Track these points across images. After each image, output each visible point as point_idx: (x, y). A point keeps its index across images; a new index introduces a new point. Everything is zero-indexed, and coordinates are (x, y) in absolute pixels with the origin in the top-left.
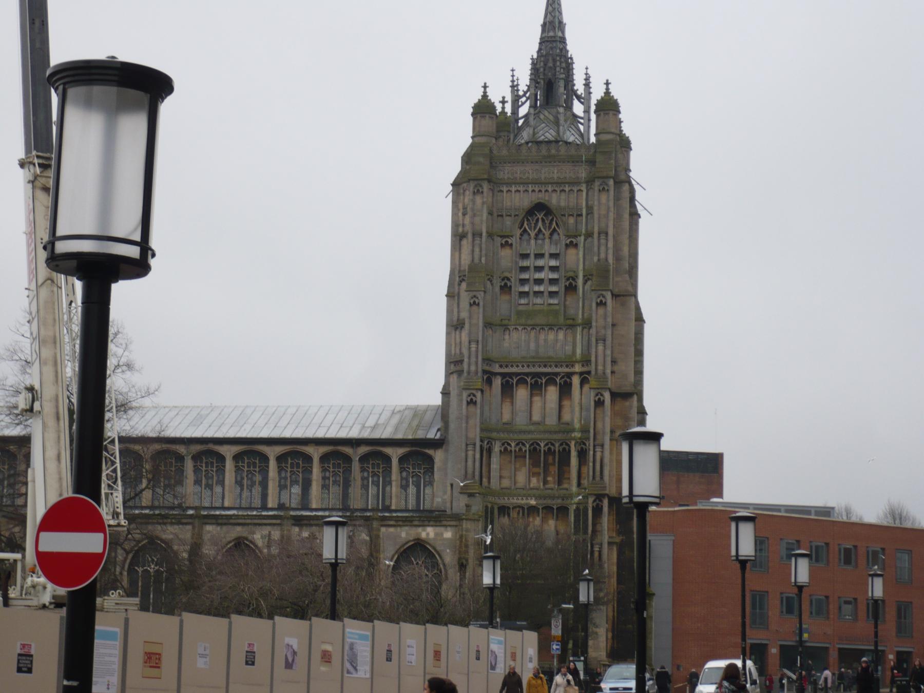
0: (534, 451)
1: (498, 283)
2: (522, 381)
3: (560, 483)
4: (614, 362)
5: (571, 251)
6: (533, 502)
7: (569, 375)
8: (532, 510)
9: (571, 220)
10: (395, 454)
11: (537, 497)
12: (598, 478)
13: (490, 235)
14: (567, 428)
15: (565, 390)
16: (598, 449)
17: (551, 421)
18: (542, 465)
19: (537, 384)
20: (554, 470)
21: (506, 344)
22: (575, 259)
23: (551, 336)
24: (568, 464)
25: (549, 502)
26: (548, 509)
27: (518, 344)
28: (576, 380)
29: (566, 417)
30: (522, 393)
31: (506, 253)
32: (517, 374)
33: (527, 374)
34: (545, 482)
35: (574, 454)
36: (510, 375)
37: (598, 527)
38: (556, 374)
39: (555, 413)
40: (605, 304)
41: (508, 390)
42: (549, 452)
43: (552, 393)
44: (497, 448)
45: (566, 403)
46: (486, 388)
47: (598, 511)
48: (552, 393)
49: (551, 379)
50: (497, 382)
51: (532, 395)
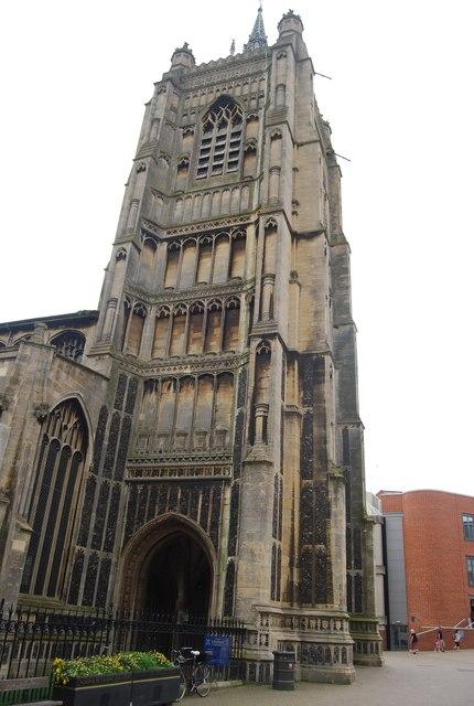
0: (196, 312)
1: (175, 163)
2: (190, 243)
3: (224, 346)
4: (295, 203)
5: (253, 125)
6: (188, 371)
7: (243, 228)
8: (186, 379)
9: (254, 103)
10: (47, 336)
11: (192, 365)
12: (266, 318)
13: (168, 123)
14: (240, 283)
15: (238, 243)
16: (267, 281)
17: (220, 278)
18: (204, 327)
19: (205, 244)
20: (218, 332)
21: (177, 213)
22: (255, 130)
23: (226, 195)
24: (237, 324)
25: (208, 369)
26: (205, 377)
27: (190, 211)
28: (251, 231)
29: (237, 273)
30: (190, 255)
31: (190, 140)
32: (183, 237)
33: (195, 235)
34: (206, 347)
35: (244, 307)
36: (177, 239)
37: (265, 383)
38: (228, 229)
39: (226, 269)
40: (280, 137)
41: (173, 253)
42: (214, 310)
43: (224, 249)
44: (152, 313)
45: (239, 259)
46: (147, 251)
47: (264, 357)
48: (224, 249)
49: (222, 236)
50: (163, 248)
51: (200, 257)
